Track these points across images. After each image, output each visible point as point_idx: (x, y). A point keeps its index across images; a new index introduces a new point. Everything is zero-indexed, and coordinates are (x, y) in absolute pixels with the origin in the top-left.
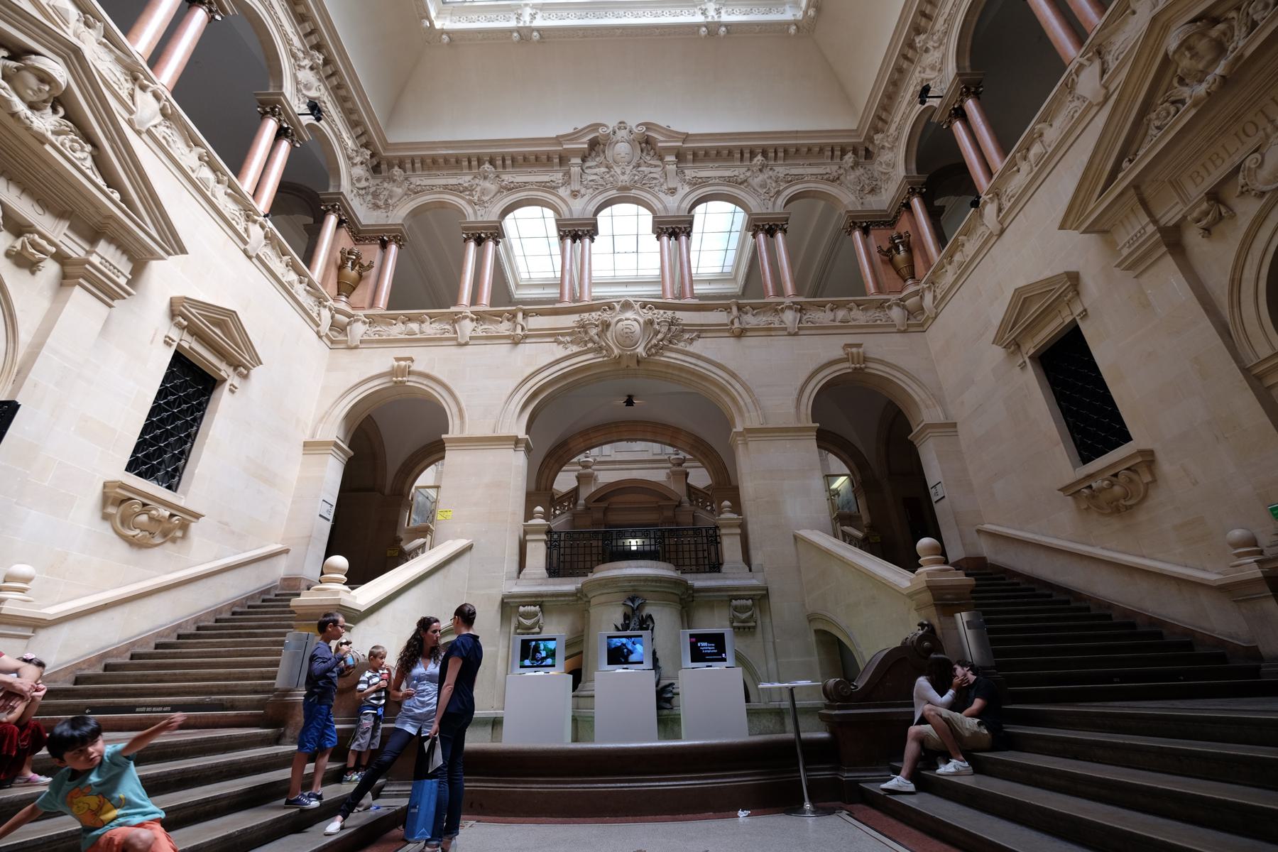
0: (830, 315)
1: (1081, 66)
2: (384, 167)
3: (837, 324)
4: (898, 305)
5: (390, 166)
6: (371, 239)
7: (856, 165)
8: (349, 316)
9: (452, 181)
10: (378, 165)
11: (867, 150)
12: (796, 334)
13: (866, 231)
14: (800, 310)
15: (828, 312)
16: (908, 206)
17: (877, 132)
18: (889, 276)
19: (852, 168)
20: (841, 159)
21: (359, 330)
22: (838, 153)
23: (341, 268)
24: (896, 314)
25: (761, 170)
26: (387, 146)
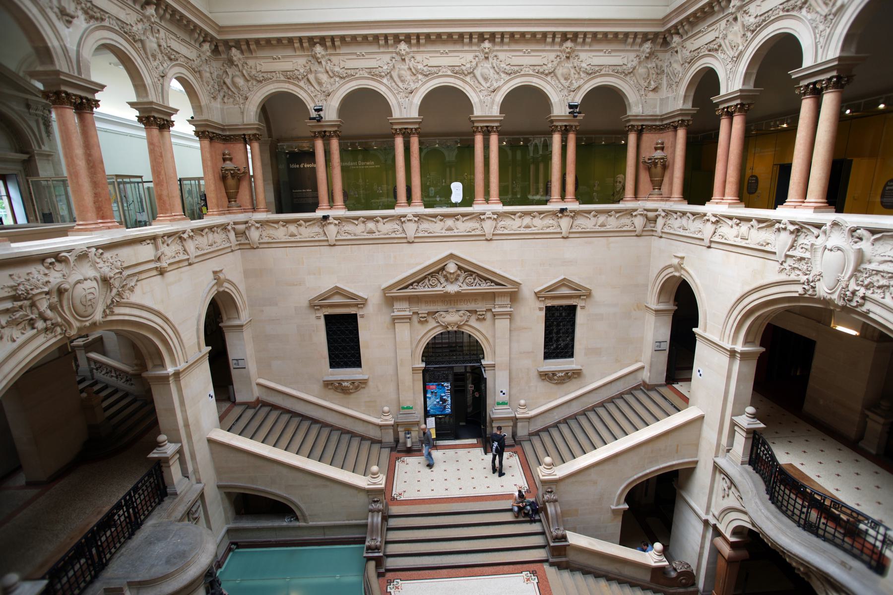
0: (593, 220)
1: (785, 229)
2: (221, 48)
3: (597, 229)
4: (641, 215)
5: (229, 48)
6: (236, 140)
7: (651, 56)
8: (246, 222)
9: (287, 65)
10: (216, 46)
11: (665, 39)
12: (567, 238)
13: (640, 132)
14: (572, 217)
15: (592, 219)
16: (675, 129)
17: (678, 33)
18: (644, 177)
19: (647, 58)
20: (641, 45)
21: (254, 234)
22: (639, 40)
23: (224, 178)
24: (639, 222)
25: (568, 58)
26: (221, 29)
